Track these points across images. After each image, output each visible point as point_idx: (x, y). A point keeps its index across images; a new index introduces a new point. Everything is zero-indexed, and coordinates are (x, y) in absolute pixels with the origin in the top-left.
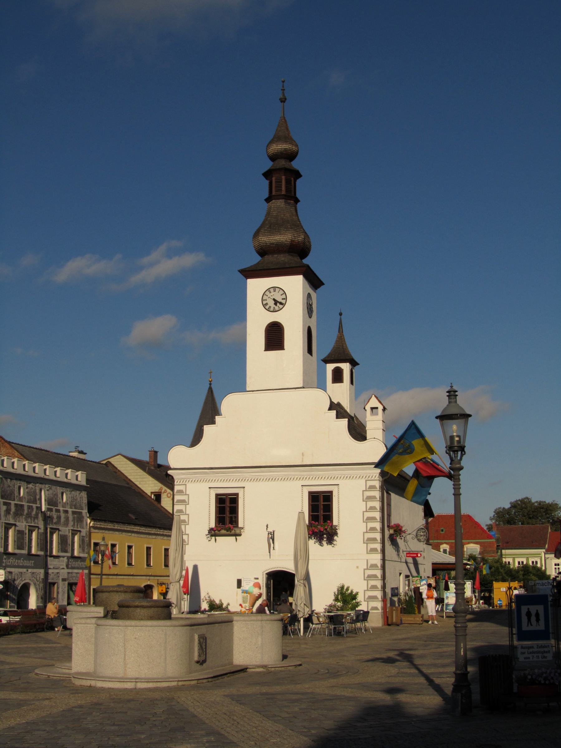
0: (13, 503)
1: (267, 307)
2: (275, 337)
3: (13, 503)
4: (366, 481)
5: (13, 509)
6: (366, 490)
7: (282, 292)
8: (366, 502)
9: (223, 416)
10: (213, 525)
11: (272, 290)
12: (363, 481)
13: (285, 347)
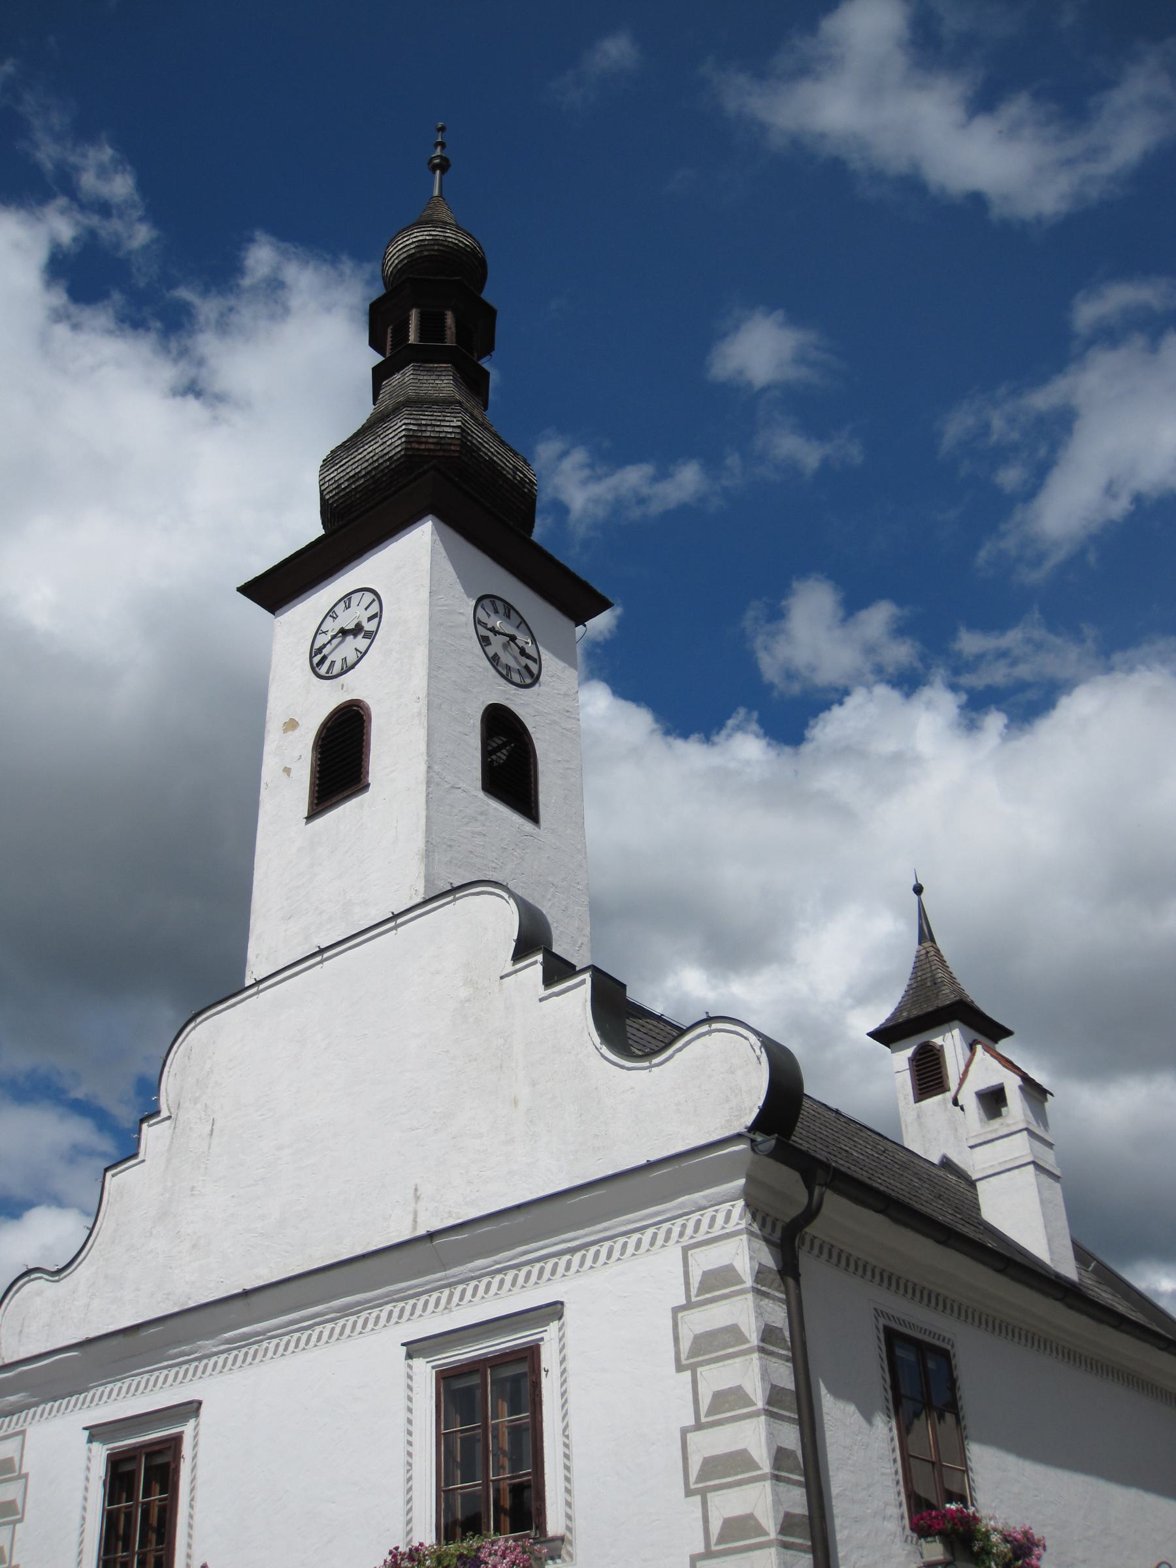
1: (323, 670)
2: (341, 758)
4: (686, 1250)
6: (689, 1306)
7: (369, 597)
8: (693, 1368)
9: (164, 1113)
12: (674, 1252)
13: (370, 780)
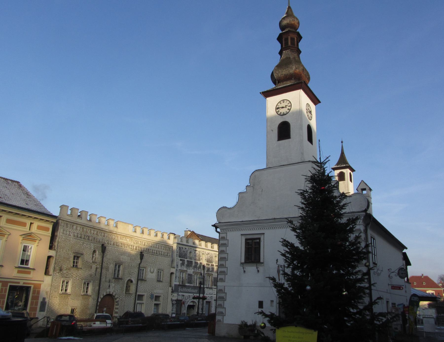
0: (186, 260)
3: (186, 260)
5: (186, 263)
7: (288, 102)
10: (243, 261)
11: (282, 102)
